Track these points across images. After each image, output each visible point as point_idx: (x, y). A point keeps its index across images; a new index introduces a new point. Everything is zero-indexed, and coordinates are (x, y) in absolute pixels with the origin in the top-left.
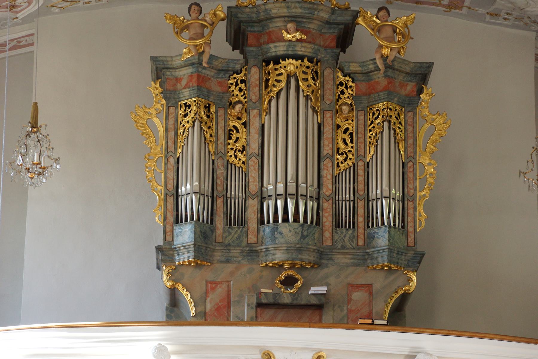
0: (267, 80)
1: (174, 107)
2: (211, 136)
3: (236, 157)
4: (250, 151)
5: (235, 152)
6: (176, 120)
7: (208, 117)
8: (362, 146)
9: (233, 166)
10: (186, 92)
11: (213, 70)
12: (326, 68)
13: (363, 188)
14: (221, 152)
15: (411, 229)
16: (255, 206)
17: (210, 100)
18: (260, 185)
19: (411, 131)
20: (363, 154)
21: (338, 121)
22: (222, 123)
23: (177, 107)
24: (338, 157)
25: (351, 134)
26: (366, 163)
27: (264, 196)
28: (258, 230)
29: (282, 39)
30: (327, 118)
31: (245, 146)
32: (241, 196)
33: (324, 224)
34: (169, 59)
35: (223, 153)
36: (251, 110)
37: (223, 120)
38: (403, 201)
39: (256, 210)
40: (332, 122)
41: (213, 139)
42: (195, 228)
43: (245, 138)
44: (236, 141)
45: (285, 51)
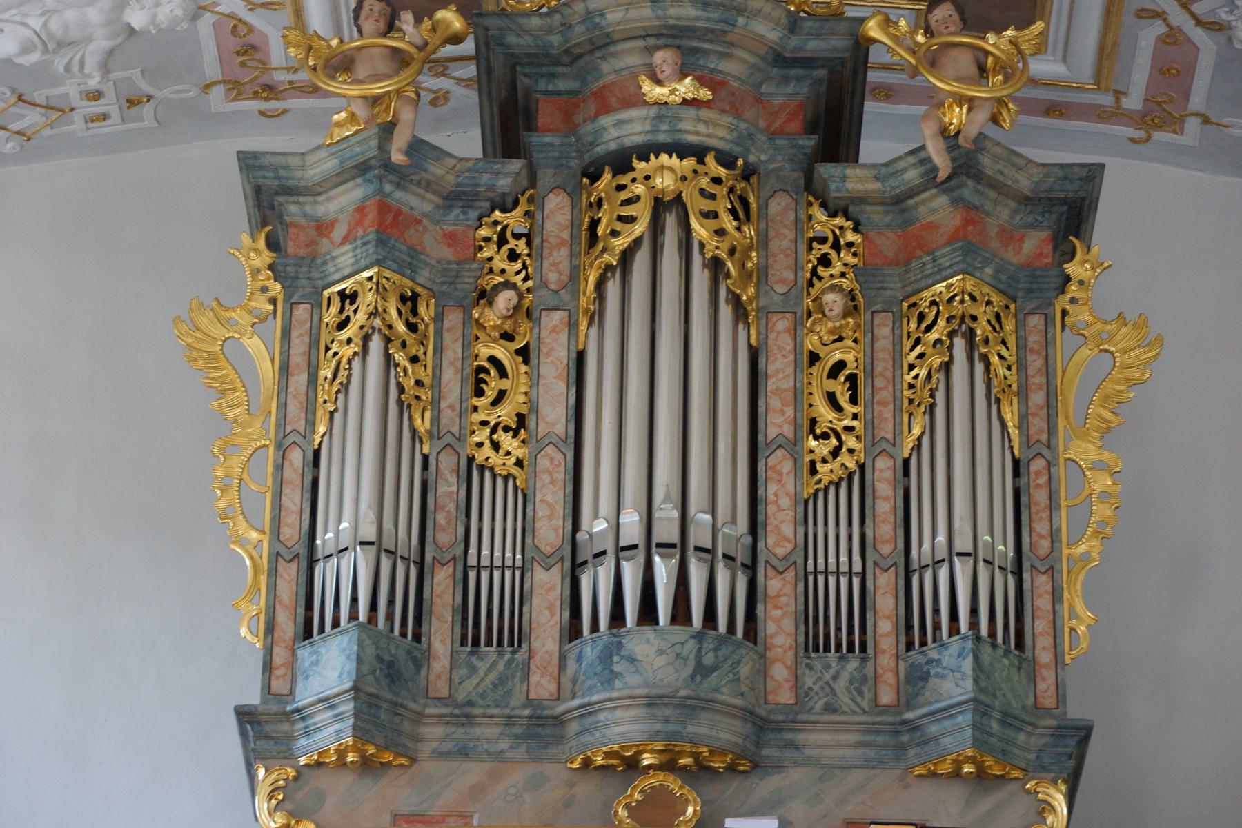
0: (595, 223)
1: (309, 306)
2: (419, 383)
3: (496, 446)
4: (539, 429)
5: (494, 431)
6: (314, 343)
7: (412, 328)
8: (888, 413)
9: (487, 475)
10: (345, 257)
11: (429, 196)
12: (775, 192)
13: (893, 534)
14: (449, 431)
15: (1045, 657)
16: (552, 588)
17: (419, 280)
18: (569, 527)
19: (1040, 370)
20: (889, 436)
21: (811, 343)
22: (453, 350)
23: (317, 304)
24: (813, 443)
25: (852, 379)
26: (899, 463)
27: (579, 560)
28: (563, 658)
29: (638, 100)
30: (779, 333)
31: (524, 415)
32: (509, 563)
33: (768, 640)
34: (294, 162)
35: (457, 436)
36: (544, 313)
37: (457, 340)
38: (1018, 574)
39: (556, 600)
40: (792, 345)
41: (426, 395)
42: (361, 644)
43: (526, 393)
44: (495, 403)
45: (648, 132)
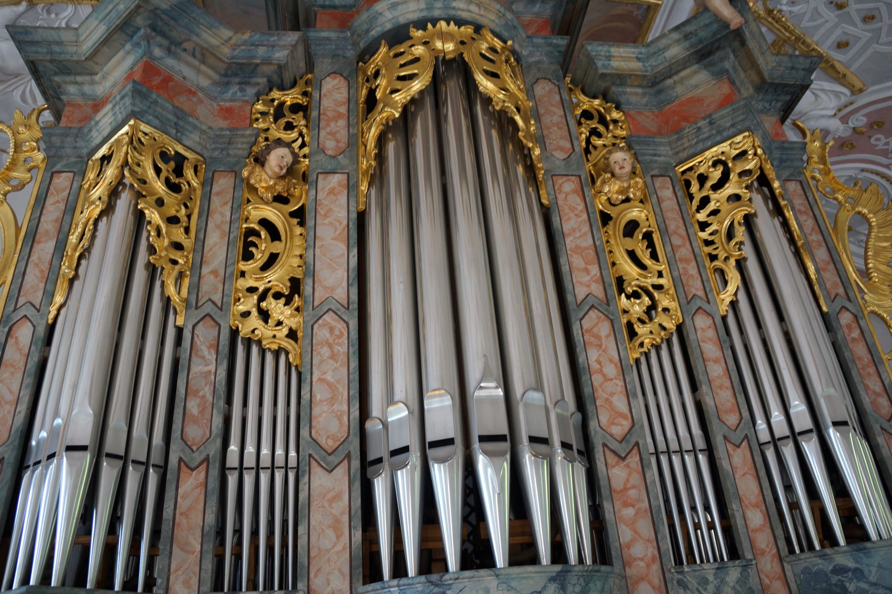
1: (71, 175)
3: (265, 315)
4: (316, 295)
5: (263, 297)
8: (692, 269)
9: (255, 350)
11: (203, 68)
12: (537, 80)
13: (734, 401)
14: (210, 300)
16: (337, 497)
17: (188, 143)
18: (355, 413)
19: (813, 229)
20: (701, 293)
21: (600, 204)
25: (648, 236)
26: (719, 321)
27: (372, 456)
30: (567, 194)
31: (299, 279)
32: (280, 461)
33: (625, 551)
34: (67, 36)
35: (219, 305)
36: (321, 177)
37: (226, 203)
39: (342, 513)
40: (583, 205)
43: (301, 256)
44: (265, 267)
45: (421, 10)
